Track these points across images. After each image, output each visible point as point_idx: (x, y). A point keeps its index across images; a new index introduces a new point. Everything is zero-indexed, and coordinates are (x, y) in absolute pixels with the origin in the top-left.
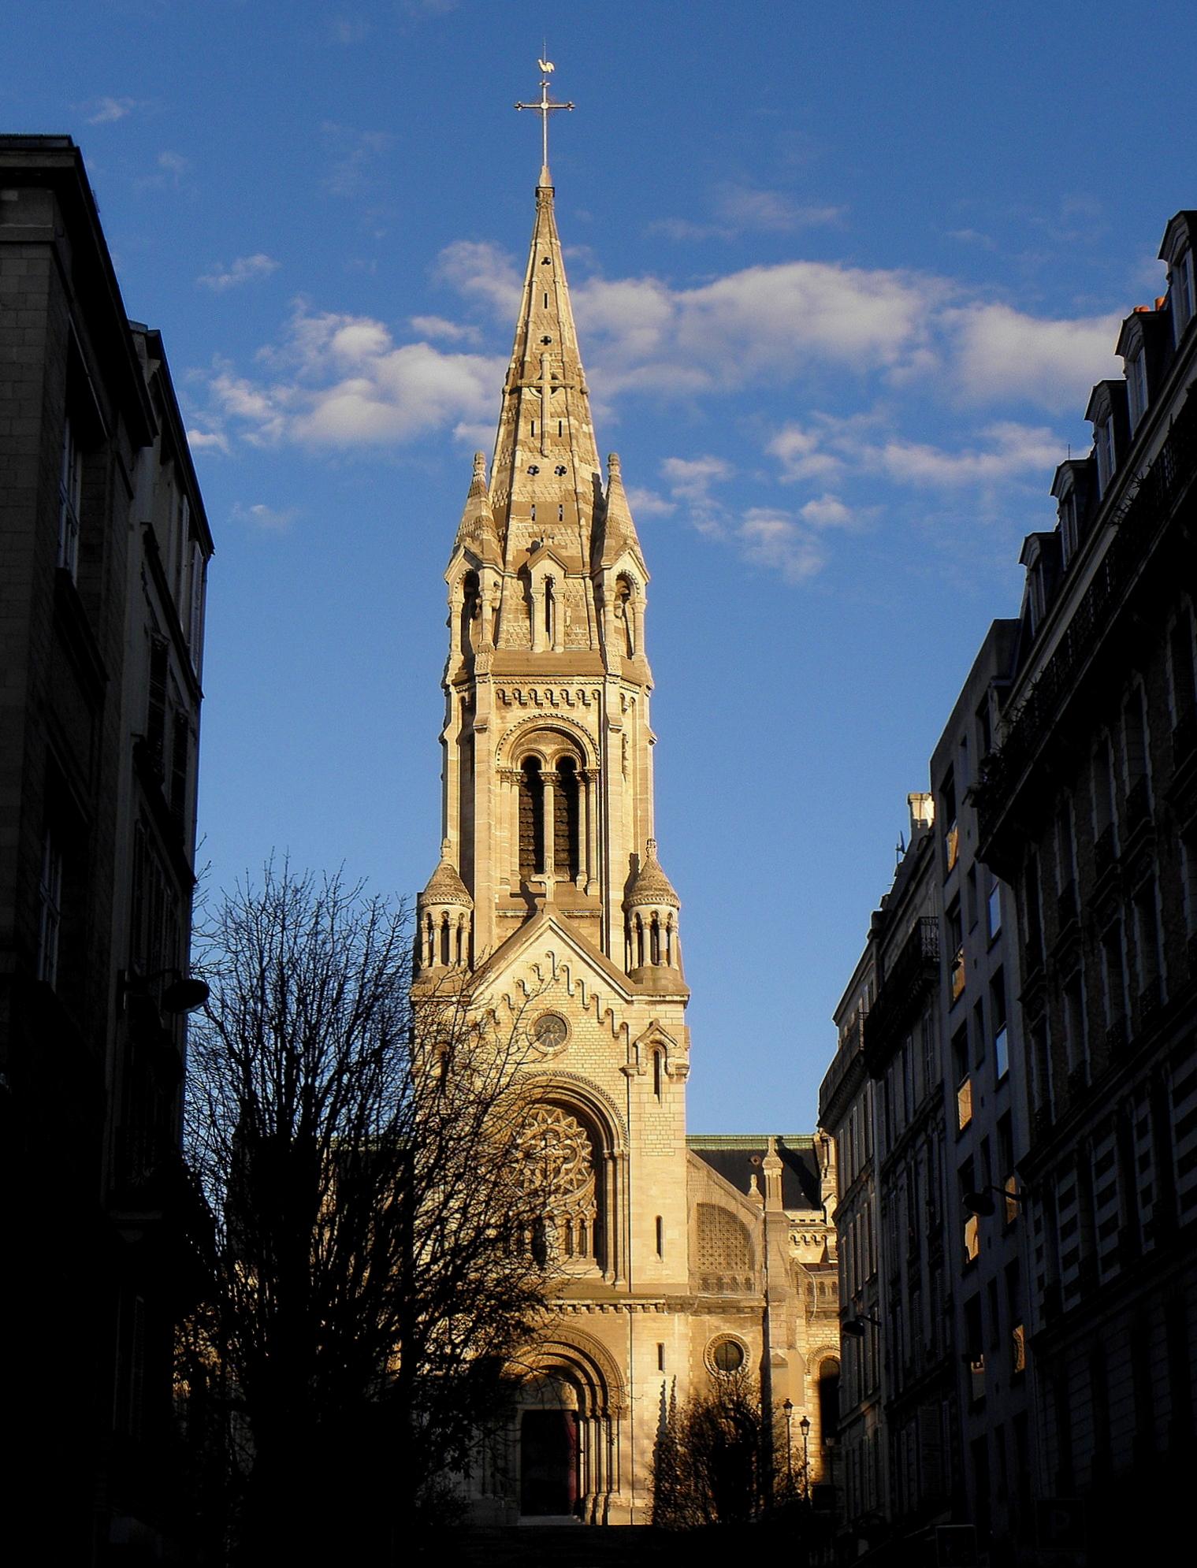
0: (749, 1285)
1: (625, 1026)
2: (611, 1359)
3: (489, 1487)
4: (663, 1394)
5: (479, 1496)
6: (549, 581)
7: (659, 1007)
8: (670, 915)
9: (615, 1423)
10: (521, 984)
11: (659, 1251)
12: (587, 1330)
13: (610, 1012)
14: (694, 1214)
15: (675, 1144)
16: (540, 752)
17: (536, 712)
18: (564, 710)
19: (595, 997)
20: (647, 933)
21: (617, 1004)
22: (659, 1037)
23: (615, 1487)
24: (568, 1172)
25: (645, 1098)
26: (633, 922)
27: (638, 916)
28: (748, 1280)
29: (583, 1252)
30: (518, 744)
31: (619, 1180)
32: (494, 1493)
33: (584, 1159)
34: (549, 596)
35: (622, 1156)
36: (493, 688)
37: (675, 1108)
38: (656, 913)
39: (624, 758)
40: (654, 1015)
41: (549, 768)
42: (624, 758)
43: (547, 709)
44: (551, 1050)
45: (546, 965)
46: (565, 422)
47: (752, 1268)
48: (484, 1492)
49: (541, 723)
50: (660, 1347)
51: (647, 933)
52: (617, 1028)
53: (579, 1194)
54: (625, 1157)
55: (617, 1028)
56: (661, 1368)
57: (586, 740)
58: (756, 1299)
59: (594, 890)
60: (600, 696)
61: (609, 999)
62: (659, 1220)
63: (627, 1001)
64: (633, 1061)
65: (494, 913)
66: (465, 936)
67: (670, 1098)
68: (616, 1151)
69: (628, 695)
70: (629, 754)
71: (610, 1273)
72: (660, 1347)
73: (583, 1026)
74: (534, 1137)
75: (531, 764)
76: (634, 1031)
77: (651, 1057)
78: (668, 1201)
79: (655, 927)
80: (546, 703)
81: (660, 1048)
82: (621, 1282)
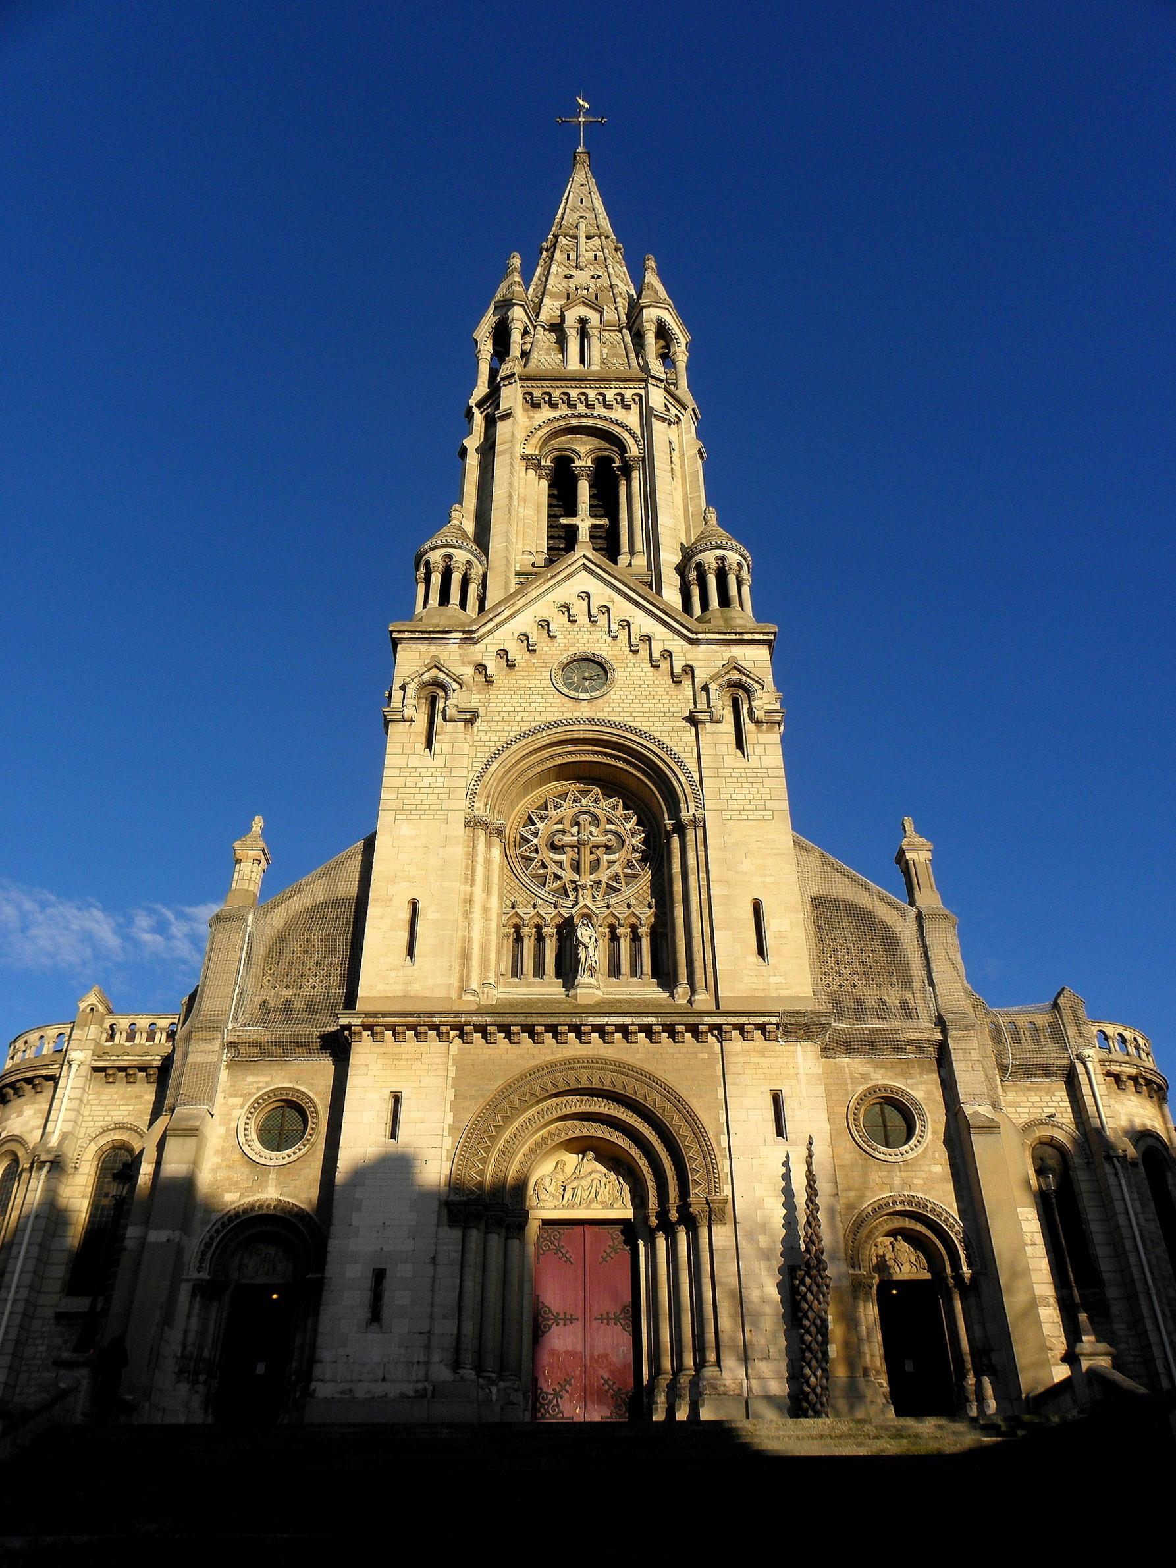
0: (907, 1011)
1: (689, 670)
2: (691, 1118)
3: (468, 1357)
4: (786, 1177)
5: (442, 1373)
6: (583, 322)
7: (737, 650)
8: (739, 564)
9: (704, 1232)
10: (545, 624)
11: (761, 952)
12: (648, 1067)
13: (668, 655)
15: (771, 805)
16: (574, 451)
17: (570, 412)
18: (602, 411)
19: (648, 639)
20: (712, 580)
21: (676, 645)
22: (736, 675)
23: (711, 1356)
24: (611, 863)
25: (723, 749)
27: (699, 566)
28: (904, 1004)
29: (636, 972)
30: (545, 442)
31: (691, 856)
32: (479, 1369)
33: (635, 849)
34: (584, 334)
36: (520, 391)
37: (767, 761)
38: (722, 559)
40: (726, 656)
43: (581, 408)
44: (585, 696)
45: (579, 608)
46: (599, 254)
47: (907, 984)
48: (456, 1366)
49: (574, 422)
50: (777, 1099)
51: (712, 580)
53: (627, 892)
54: (699, 824)
55: (677, 670)
57: (626, 435)
58: (923, 1029)
59: (640, 561)
60: (639, 399)
61: (663, 638)
62: (757, 907)
63: (691, 641)
64: (702, 705)
66: (473, 589)
67: (759, 750)
68: (685, 816)
70: (676, 459)
71: (682, 989)
72: (777, 1099)
73: (630, 670)
74: (561, 821)
76: (701, 675)
77: (728, 702)
78: (770, 879)
79: (722, 575)
81: (741, 692)
82: (703, 999)
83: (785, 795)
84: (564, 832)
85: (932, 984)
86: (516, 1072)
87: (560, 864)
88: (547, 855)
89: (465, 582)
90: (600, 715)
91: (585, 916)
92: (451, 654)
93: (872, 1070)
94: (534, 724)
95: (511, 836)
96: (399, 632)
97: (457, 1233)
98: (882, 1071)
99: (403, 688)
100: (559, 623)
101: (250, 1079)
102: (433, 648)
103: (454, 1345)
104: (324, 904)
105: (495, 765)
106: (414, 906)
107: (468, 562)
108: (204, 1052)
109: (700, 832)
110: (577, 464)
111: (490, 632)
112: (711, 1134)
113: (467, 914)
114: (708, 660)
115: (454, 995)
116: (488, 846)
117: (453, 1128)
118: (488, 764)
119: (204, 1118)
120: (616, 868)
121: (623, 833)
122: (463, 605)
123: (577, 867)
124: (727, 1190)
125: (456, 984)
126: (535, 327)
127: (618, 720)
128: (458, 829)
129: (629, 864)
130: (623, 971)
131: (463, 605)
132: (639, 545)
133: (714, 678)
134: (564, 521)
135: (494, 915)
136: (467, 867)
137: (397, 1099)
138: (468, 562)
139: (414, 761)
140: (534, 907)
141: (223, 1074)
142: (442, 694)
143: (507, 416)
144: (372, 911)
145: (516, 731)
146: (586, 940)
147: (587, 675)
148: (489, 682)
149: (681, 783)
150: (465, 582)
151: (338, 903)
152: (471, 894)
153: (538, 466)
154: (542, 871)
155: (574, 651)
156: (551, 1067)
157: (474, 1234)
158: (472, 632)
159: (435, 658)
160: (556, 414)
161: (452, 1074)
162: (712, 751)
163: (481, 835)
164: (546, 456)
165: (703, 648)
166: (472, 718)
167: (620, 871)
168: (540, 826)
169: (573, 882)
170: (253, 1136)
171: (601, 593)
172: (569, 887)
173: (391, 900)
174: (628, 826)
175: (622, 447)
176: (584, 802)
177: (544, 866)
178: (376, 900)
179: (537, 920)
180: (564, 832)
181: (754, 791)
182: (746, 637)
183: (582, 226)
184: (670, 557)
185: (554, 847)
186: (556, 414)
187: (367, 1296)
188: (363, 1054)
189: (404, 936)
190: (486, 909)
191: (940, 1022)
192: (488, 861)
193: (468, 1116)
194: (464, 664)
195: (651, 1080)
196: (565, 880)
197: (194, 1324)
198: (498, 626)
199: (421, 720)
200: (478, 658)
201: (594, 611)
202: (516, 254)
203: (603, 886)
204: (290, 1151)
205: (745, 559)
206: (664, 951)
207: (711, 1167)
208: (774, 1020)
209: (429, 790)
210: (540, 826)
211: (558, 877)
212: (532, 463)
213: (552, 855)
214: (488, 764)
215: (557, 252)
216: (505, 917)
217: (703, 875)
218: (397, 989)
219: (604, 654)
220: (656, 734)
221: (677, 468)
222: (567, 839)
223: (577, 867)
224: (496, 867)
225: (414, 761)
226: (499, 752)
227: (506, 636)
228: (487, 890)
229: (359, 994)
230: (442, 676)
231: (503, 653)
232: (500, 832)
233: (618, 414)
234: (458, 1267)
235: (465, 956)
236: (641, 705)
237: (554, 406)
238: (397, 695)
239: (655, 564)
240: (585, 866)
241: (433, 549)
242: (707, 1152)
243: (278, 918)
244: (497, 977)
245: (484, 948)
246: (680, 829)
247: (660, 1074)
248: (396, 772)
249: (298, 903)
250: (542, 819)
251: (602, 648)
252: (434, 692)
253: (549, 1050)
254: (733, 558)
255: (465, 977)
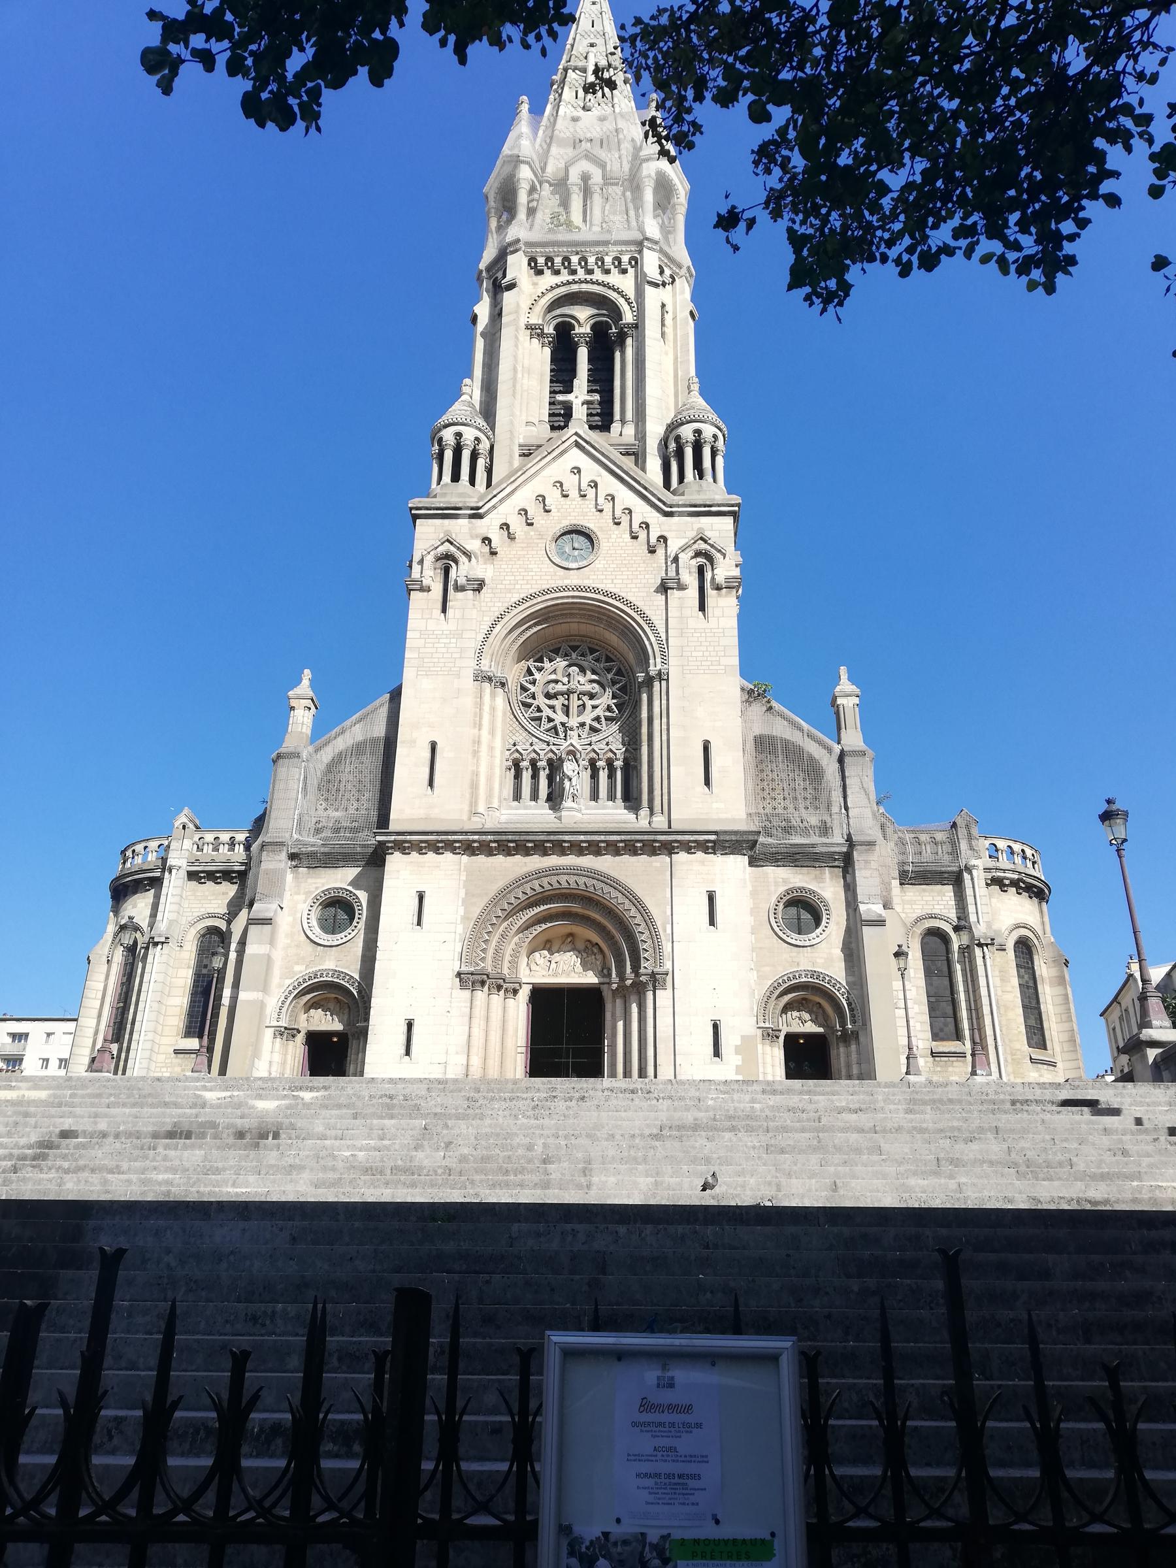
1: (663, 539)
6: (585, 178)
8: (715, 436)
9: (650, 995)
10: (542, 499)
11: (707, 782)
12: (614, 874)
14: (750, 745)
15: (724, 661)
17: (571, 278)
18: (598, 275)
20: (689, 452)
21: (653, 517)
22: (702, 546)
24: (594, 707)
25: (687, 612)
26: (672, 446)
27: (678, 439)
29: (612, 797)
35: (660, 673)
36: (525, 261)
38: (698, 432)
39: (663, 325)
40: (696, 526)
41: (583, 329)
42: (663, 325)
43: (581, 274)
45: (571, 482)
49: (575, 288)
51: (689, 452)
52: (653, 540)
55: (653, 540)
56: (712, 922)
57: (621, 302)
59: (629, 430)
60: (635, 262)
64: (672, 574)
65: (517, 452)
66: (481, 463)
67: (718, 612)
68: (653, 670)
69: (667, 272)
71: (644, 812)
73: (613, 540)
74: (554, 672)
75: (564, 332)
76: (674, 546)
80: (581, 272)
83: (737, 652)
84: (556, 682)
85: (847, 809)
86: (511, 877)
87: (552, 707)
88: (541, 701)
89: (474, 456)
90: (587, 583)
91: (570, 753)
92: (460, 528)
93: (791, 876)
94: (532, 591)
95: (512, 685)
96: (417, 509)
97: (467, 994)
98: (800, 876)
99: (421, 562)
100: (553, 497)
101: (310, 880)
102: (446, 521)
103: (464, 1072)
104: (364, 742)
105: (498, 628)
106: (434, 747)
107: (477, 439)
108: (274, 863)
109: (664, 683)
110: (577, 331)
111: (494, 507)
112: (659, 924)
113: (476, 753)
114: (680, 532)
115: (465, 817)
116: (493, 695)
117: (465, 918)
118: (493, 626)
119: (276, 911)
120: (599, 712)
121: (605, 683)
122: (472, 482)
123: (566, 710)
124: (668, 966)
125: (466, 808)
126: (541, 184)
127: (601, 586)
128: (468, 682)
129: (609, 709)
130: (601, 796)
131: (472, 482)
132: (629, 415)
133: (683, 549)
134: (560, 397)
135: (498, 753)
136: (475, 714)
137: (421, 897)
138: (477, 439)
139: (432, 625)
140: (531, 745)
141: (289, 877)
142: (453, 564)
143: (512, 286)
144: (401, 751)
145: (516, 597)
146: (569, 773)
147: (576, 545)
148: (493, 553)
149: (651, 643)
150: (474, 456)
151: (374, 741)
152: (479, 736)
153: (541, 335)
154: (538, 714)
155: (566, 523)
156: (539, 874)
157: (481, 995)
158: (478, 508)
159: (447, 533)
160: (557, 280)
161: (464, 878)
162: (678, 614)
163: (486, 685)
164: (549, 323)
165: (676, 519)
166: (479, 586)
167: (601, 714)
168: (537, 676)
169: (563, 724)
170: (314, 923)
171: (591, 470)
172: (559, 727)
173: (415, 742)
174: (609, 676)
175: (616, 313)
176: (574, 655)
177: (539, 710)
178: (403, 742)
179: (534, 755)
180: (556, 682)
181: (711, 649)
182: (713, 509)
183: (591, 58)
184: (655, 430)
185: (548, 696)
186: (557, 280)
187: (403, 1038)
188: (395, 863)
189: (427, 770)
190: (491, 748)
191: (849, 838)
192: (493, 709)
193: (476, 911)
194: (472, 537)
195: (615, 884)
196: (557, 722)
197: (277, 1058)
198: (501, 501)
199: (437, 588)
200: (484, 532)
201: (584, 485)
202: (525, 98)
203: (587, 727)
204: (342, 935)
205: (720, 430)
206: (630, 780)
207: (657, 948)
208: (713, 837)
209: (444, 650)
210: (537, 676)
211: (550, 720)
212: (535, 331)
213: (548, 702)
214: (493, 626)
215: (566, 88)
216: (508, 753)
217: (664, 720)
218: (420, 813)
219: (591, 526)
220: (631, 599)
221: (669, 330)
222: (560, 687)
223: (566, 710)
224: (499, 714)
225: (432, 625)
226: (501, 616)
227: (507, 511)
228: (492, 732)
229: (392, 816)
230: (453, 549)
231: (505, 526)
232: (503, 685)
233: (615, 278)
234: (467, 1018)
235: (474, 786)
236: (620, 574)
237: (557, 273)
238: (416, 568)
239: (641, 435)
240: (574, 709)
241: (446, 426)
242: (655, 935)
243: (327, 755)
244: (500, 802)
245: (490, 779)
246: (649, 682)
247: (622, 879)
248: (417, 635)
249: (342, 743)
250: (540, 670)
251: (591, 522)
252: (446, 562)
253: (536, 862)
254: (708, 431)
255: (473, 802)
